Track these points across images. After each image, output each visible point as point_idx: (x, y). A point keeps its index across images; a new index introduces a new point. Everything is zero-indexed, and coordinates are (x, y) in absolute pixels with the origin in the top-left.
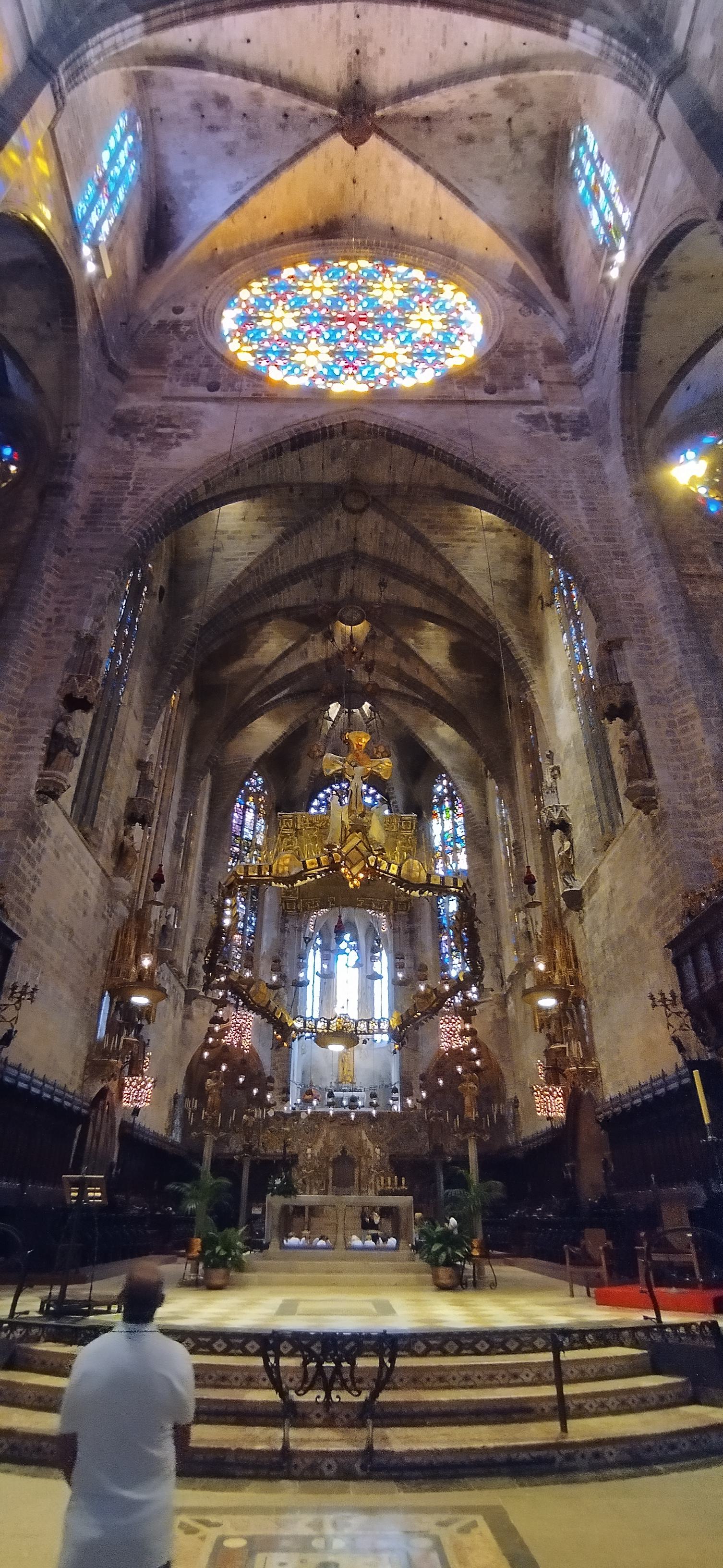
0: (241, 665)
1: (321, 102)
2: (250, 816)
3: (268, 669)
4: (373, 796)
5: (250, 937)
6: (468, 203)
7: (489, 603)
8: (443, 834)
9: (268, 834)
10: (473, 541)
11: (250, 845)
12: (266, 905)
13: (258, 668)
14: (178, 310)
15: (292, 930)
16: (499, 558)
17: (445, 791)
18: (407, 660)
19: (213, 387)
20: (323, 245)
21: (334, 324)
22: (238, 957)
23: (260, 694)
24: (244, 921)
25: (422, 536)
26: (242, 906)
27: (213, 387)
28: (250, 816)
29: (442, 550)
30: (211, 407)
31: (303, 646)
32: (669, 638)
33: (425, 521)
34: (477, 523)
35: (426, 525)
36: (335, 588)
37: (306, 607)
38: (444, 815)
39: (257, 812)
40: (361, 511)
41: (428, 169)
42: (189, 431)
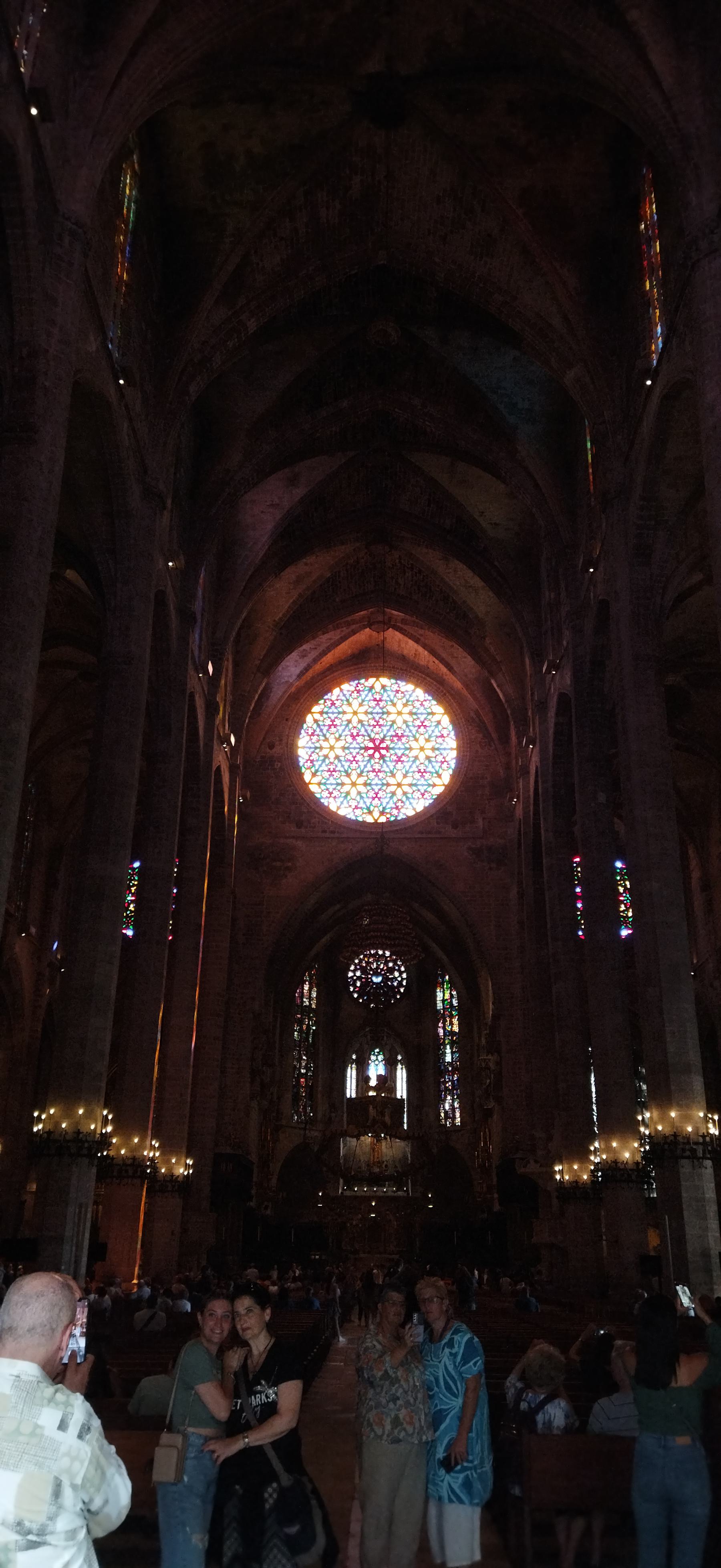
1: (357, 623)
2: (306, 987)
5: (310, 1079)
6: (450, 668)
8: (443, 1001)
14: (271, 747)
19: (299, 825)
20: (358, 668)
21: (366, 754)
22: (304, 1094)
24: (306, 1067)
26: (304, 1058)
27: (299, 825)
28: (306, 987)
30: (299, 843)
38: (445, 986)
41: (425, 646)
42: (290, 864)
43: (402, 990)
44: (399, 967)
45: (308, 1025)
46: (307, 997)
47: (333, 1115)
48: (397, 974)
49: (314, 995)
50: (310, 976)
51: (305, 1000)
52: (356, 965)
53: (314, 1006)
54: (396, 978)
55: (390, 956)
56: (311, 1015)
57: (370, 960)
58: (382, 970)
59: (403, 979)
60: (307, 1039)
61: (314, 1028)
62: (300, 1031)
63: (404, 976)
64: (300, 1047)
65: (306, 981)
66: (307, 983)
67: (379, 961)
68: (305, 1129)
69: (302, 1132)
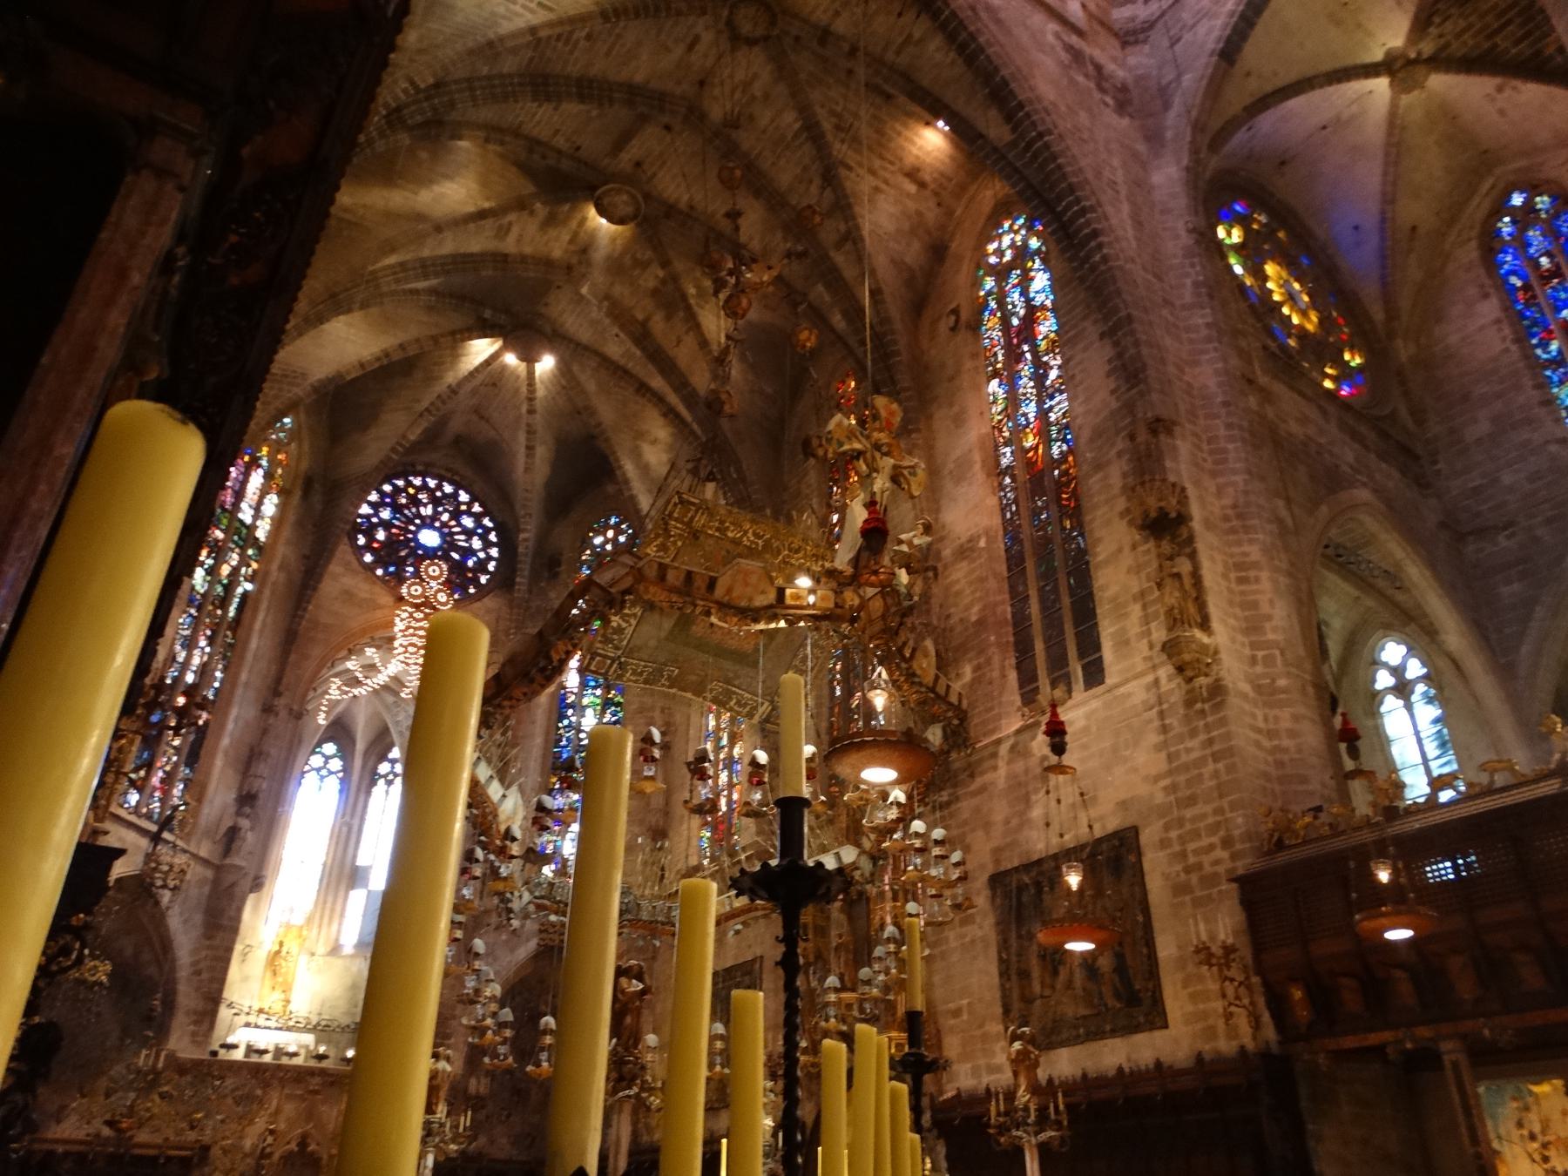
0: (396, 198)
2: (256, 479)
3: (438, 229)
4: (478, 518)
7: (883, 286)
9: (278, 522)
10: (886, 182)
11: (245, 536)
12: (249, 656)
13: (420, 217)
15: (283, 714)
16: (906, 226)
17: (609, 547)
18: (668, 318)
23: (402, 265)
25: (822, 135)
28: (256, 479)
29: (843, 172)
31: (512, 217)
32: (1231, 446)
33: (833, 113)
34: (901, 159)
35: (834, 120)
36: (619, 145)
37: (559, 152)
39: (269, 476)
40: (751, 42)
43: (483, 579)
44: (487, 531)
45: (235, 571)
46: (253, 504)
47: (244, 823)
48: (477, 543)
49: (271, 505)
50: (273, 461)
51: (244, 505)
52: (383, 494)
53: (261, 534)
54: (473, 552)
55: (470, 504)
56: (250, 552)
57: (420, 496)
58: (444, 525)
59: (490, 558)
60: (224, 603)
61: (249, 586)
62: (212, 572)
63: (494, 552)
64: (199, 609)
65: (260, 466)
66: (261, 472)
67: (442, 505)
68: (156, 838)
69: (144, 843)
